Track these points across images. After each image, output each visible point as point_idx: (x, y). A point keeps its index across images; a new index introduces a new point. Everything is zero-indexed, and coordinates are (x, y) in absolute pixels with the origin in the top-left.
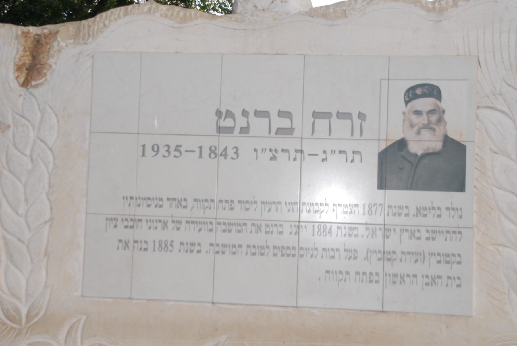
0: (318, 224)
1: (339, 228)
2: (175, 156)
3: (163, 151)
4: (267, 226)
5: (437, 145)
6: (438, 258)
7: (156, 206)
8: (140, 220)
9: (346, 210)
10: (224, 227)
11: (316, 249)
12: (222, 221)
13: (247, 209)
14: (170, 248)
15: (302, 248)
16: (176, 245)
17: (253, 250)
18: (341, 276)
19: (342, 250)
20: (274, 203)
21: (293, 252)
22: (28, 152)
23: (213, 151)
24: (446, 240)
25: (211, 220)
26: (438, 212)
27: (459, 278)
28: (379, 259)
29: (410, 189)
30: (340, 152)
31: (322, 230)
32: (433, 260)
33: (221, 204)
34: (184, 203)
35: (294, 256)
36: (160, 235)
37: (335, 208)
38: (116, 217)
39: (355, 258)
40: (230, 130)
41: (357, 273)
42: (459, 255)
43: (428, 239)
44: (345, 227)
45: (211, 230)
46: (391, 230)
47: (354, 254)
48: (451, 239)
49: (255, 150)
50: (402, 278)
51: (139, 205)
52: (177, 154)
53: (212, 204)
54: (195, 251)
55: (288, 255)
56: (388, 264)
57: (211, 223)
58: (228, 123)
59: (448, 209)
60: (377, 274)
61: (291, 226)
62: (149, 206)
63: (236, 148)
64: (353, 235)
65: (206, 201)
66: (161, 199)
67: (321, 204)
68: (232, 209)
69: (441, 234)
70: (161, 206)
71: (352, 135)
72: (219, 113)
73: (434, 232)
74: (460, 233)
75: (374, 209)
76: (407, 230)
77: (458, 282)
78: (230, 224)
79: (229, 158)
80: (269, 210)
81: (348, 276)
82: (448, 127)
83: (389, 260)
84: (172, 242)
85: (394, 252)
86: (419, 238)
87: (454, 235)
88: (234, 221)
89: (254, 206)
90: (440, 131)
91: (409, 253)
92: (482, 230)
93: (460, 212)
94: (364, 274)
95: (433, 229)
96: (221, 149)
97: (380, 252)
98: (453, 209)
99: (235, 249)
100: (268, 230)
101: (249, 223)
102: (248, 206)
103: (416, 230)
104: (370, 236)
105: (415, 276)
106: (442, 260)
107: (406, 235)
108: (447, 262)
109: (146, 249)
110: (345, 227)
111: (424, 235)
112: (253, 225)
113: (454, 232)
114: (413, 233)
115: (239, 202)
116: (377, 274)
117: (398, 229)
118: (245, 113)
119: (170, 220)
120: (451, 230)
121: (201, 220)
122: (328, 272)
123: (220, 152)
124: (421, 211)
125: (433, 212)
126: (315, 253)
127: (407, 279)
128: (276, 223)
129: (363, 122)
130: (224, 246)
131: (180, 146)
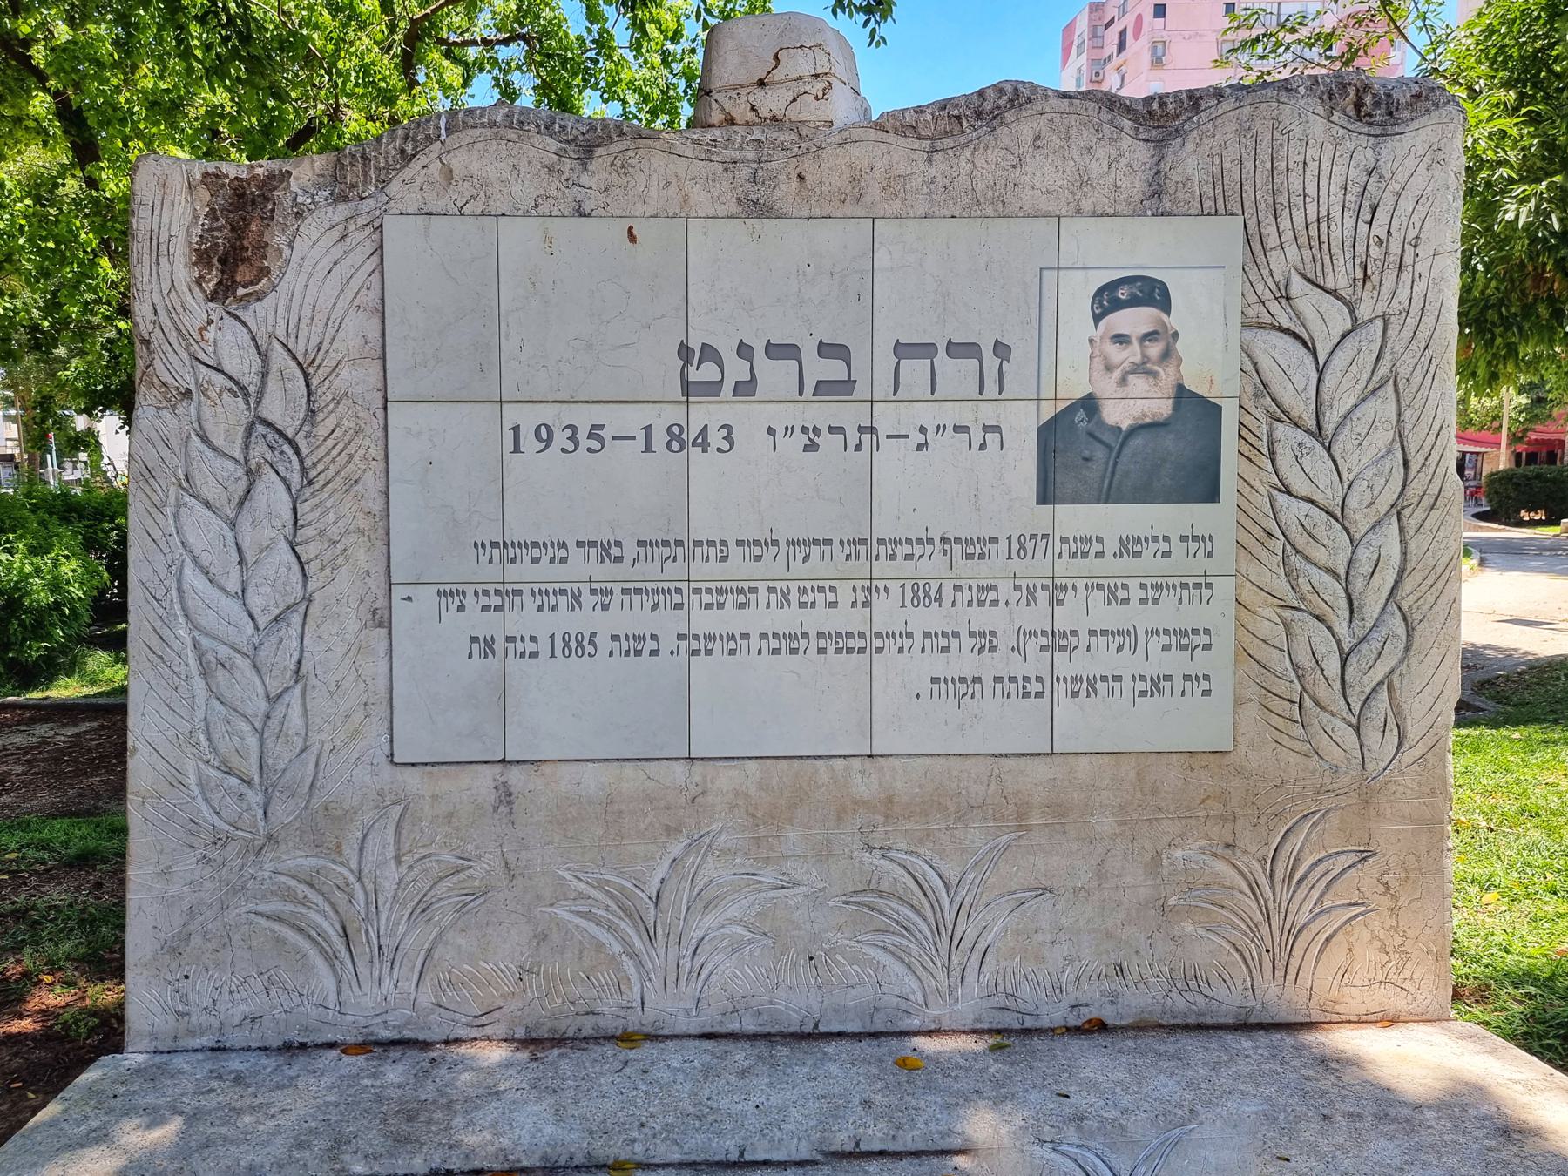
1: (957, 588)
2: (589, 450)
4: (802, 591)
6: (1165, 640)
10: (707, 598)
11: (910, 635)
12: (702, 585)
13: (757, 558)
15: (878, 635)
16: (603, 642)
17: (774, 644)
19: (964, 634)
20: (816, 542)
21: (861, 643)
23: (676, 437)
25: (678, 585)
26: (1164, 547)
28: (1043, 649)
31: (921, 594)
32: (1155, 644)
33: (698, 550)
35: (862, 650)
36: (566, 621)
37: (947, 547)
39: (993, 649)
41: (998, 680)
43: (1143, 602)
44: (970, 588)
45: (679, 606)
47: (991, 641)
50: (1092, 684)
52: (595, 445)
53: (680, 550)
54: (646, 652)
55: (850, 651)
57: (679, 591)
59: (1184, 539)
60: (1039, 679)
61: (854, 589)
64: (988, 603)
65: (666, 543)
66: (563, 545)
67: (919, 541)
68: (724, 559)
70: (563, 560)
72: (684, 352)
73: (1155, 587)
74: (1209, 586)
75: (1029, 545)
76: (1100, 587)
77: (1204, 685)
78: (721, 591)
79: (712, 449)
80: (806, 558)
81: (977, 686)
83: (1063, 649)
84: (593, 634)
85: (1074, 633)
86: (1125, 602)
91: (1104, 632)
94: (1013, 679)
97: (1044, 633)
98: (1195, 538)
99: (733, 642)
100: (804, 599)
101: (763, 588)
102: (758, 551)
104: (1024, 600)
105: (1118, 679)
106: (1174, 643)
107: (1098, 595)
108: (1184, 647)
111: (1136, 594)
112: (771, 590)
113: (1197, 586)
114: (1112, 592)
115: (739, 543)
116: (1039, 679)
117: (1081, 584)
118: (744, 351)
119: (585, 588)
120: (1190, 581)
122: (935, 680)
123: (691, 440)
124: (1129, 546)
125: (1153, 546)
126: (907, 642)
128: (821, 584)
130: (709, 637)
131: (601, 427)
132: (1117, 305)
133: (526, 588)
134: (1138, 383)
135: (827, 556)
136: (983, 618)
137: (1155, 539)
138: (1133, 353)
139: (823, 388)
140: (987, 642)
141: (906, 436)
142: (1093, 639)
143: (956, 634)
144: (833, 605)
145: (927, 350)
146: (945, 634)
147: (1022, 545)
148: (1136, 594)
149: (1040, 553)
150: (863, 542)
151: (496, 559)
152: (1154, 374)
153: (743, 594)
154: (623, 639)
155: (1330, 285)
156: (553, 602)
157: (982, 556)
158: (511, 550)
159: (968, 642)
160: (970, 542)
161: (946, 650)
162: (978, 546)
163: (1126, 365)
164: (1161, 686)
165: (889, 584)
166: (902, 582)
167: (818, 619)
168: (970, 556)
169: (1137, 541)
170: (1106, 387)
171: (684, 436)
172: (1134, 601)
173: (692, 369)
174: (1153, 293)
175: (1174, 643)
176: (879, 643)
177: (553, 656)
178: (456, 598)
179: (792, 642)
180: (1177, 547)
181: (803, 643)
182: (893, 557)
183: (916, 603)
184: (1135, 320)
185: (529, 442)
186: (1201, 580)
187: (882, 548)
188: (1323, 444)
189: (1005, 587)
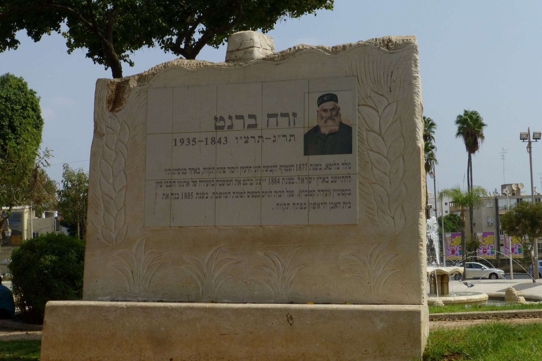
0: (272, 177)
1: (283, 179)
2: (193, 145)
3: (186, 142)
4: (244, 181)
5: (336, 128)
6: (338, 192)
7: (183, 173)
8: (174, 182)
9: (287, 169)
10: (220, 183)
11: (271, 192)
12: (219, 179)
13: (233, 172)
14: (191, 197)
15: (263, 192)
16: (195, 195)
17: (237, 195)
18: (285, 206)
20: (247, 167)
21: (258, 194)
22: (113, 148)
23: (213, 140)
24: (342, 182)
26: (338, 166)
27: (350, 203)
28: (306, 195)
29: (322, 155)
30: (283, 136)
31: (274, 181)
33: (218, 170)
34: (198, 171)
36: (186, 189)
37: (281, 168)
38: (161, 181)
39: (293, 196)
40: (222, 128)
41: (294, 204)
42: (349, 190)
43: (332, 182)
45: (213, 185)
46: (312, 178)
47: (292, 194)
48: (345, 181)
49: (237, 138)
51: (174, 174)
52: (194, 143)
56: (311, 198)
57: (213, 181)
58: (221, 123)
59: (343, 164)
60: (305, 204)
62: (179, 173)
63: (226, 138)
64: (291, 183)
65: (210, 168)
66: (185, 169)
67: (274, 166)
69: (340, 179)
70: (186, 173)
71: (289, 126)
72: (216, 119)
73: (336, 178)
74: (350, 177)
75: (302, 167)
76: (321, 178)
77: (349, 205)
78: (224, 181)
79: (222, 143)
80: (245, 172)
81: (289, 206)
82: (341, 117)
83: (311, 195)
84: (192, 193)
85: (314, 191)
86: (327, 182)
87: (347, 179)
88: (226, 179)
89: (237, 170)
90: (337, 120)
91: (322, 191)
92: (362, 175)
93: (349, 165)
94: (298, 204)
95: (335, 176)
96: (218, 139)
97: (306, 191)
98: (346, 164)
100: (244, 183)
101: (234, 180)
102: (233, 170)
103: (326, 177)
104: (301, 182)
105: (326, 203)
106: (340, 193)
107: (320, 180)
108: (343, 194)
109: (178, 198)
110: (287, 179)
111: (330, 180)
113: (347, 177)
114: (324, 179)
115: (228, 168)
116: (305, 204)
117: (315, 177)
118: (230, 118)
119: (190, 181)
120: (345, 176)
121: (207, 180)
122: (277, 204)
123: (217, 141)
124: (328, 167)
125: (335, 166)
126: (270, 194)
127: (321, 206)
128: (249, 178)
129: (295, 118)
130: (220, 193)
131: (195, 139)
132: (324, 101)
133: (176, 181)
134: (330, 122)
135: (250, 171)
136: (290, 187)
137: (335, 164)
138: (328, 114)
139: (250, 126)
140: (291, 194)
141: (270, 138)
142: (319, 192)
143: (283, 192)
144: (252, 184)
145: (275, 116)
146: (280, 192)
147: (300, 167)
148: (330, 180)
149: (305, 169)
150: (259, 167)
151: (170, 173)
152: (334, 120)
153: (229, 182)
154: (199, 194)
155: (381, 94)
156: (183, 184)
157: (290, 170)
158: (173, 171)
159: (286, 194)
160: (287, 166)
161: (280, 196)
162: (289, 167)
163: (327, 117)
164: (337, 205)
165: (266, 178)
166: (269, 178)
167: (248, 188)
168: (286, 170)
169: (330, 165)
170: (321, 123)
171: (215, 140)
172: (330, 182)
173: (218, 123)
174: (333, 98)
175: (340, 193)
176: (263, 194)
177: (182, 199)
178: (160, 184)
179: (241, 194)
180: (341, 166)
181: (244, 195)
182: (267, 171)
183: (273, 183)
184: (328, 105)
185: (178, 143)
186: (348, 175)
187: (264, 168)
188: (381, 137)
189: (296, 179)
